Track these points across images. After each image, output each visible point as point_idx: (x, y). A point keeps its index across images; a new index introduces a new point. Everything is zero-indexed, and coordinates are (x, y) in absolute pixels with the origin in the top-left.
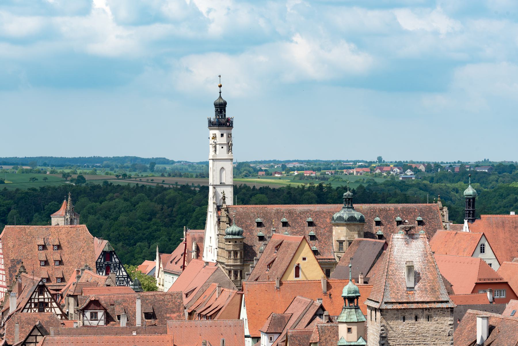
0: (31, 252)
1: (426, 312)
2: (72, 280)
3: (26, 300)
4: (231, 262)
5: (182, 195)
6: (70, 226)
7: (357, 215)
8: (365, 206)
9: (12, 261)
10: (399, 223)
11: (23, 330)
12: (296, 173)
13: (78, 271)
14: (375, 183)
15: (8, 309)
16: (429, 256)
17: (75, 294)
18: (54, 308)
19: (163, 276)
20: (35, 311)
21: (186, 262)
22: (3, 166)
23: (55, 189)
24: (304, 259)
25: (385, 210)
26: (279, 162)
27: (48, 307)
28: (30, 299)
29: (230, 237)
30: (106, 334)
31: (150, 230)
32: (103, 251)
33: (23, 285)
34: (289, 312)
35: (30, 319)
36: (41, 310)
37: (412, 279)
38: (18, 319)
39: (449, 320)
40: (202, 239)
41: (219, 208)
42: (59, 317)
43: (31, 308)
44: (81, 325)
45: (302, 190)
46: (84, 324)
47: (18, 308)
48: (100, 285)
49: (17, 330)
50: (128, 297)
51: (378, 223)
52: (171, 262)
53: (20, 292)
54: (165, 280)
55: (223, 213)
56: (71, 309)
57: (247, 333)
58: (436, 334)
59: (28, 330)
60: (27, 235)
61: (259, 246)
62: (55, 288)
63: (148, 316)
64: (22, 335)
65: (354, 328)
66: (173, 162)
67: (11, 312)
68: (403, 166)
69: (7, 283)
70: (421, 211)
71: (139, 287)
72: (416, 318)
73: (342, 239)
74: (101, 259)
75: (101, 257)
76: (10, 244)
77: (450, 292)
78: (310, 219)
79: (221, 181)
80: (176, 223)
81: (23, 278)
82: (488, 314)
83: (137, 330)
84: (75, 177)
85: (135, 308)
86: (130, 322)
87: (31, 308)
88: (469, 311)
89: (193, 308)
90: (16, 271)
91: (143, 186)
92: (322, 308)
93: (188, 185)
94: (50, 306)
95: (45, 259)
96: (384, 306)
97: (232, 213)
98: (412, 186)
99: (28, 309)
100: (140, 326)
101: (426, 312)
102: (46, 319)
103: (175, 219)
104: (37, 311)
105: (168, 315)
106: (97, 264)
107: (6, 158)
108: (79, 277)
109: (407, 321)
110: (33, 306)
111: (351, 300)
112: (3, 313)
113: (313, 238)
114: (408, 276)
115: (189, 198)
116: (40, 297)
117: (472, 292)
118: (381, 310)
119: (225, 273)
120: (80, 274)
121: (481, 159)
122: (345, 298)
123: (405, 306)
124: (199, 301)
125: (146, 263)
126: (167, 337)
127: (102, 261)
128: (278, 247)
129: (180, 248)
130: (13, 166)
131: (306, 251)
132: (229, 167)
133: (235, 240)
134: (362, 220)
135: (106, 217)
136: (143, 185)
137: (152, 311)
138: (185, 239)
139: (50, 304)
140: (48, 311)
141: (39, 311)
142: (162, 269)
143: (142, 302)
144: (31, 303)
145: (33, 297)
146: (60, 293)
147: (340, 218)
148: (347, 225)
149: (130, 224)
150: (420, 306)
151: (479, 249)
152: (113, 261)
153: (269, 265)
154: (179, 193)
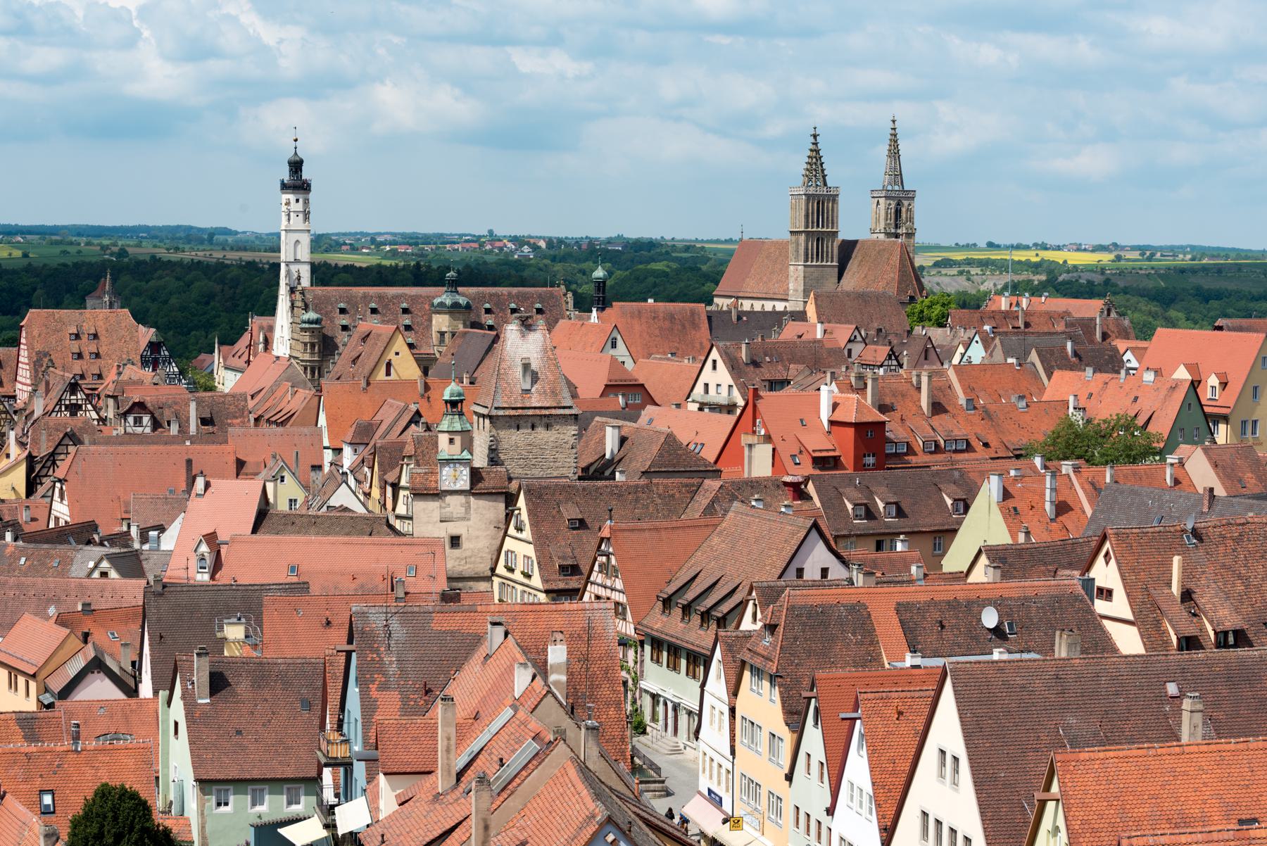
1: (546, 420)
2: (111, 376)
3: (55, 401)
4: (307, 357)
7: (462, 301)
8: (472, 290)
9: (38, 353)
10: (514, 311)
12: (388, 248)
13: (119, 366)
14: (485, 263)
16: (550, 352)
23: (90, 265)
24: (397, 354)
25: (496, 295)
26: (366, 234)
28: (60, 400)
29: (307, 326)
30: (153, 443)
34: (378, 418)
36: (73, 414)
37: (529, 379)
39: (572, 430)
40: (271, 329)
41: (292, 291)
45: (395, 269)
48: (146, 383)
49: (44, 438)
51: (488, 311)
53: (48, 391)
55: (298, 296)
56: (110, 414)
57: (326, 443)
58: (557, 447)
61: (341, 338)
63: (205, 421)
65: (458, 439)
66: (236, 233)
67: (36, 416)
68: (519, 241)
70: (540, 296)
71: (194, 387)
72: (533, 427)
73: (444, 329)
76: (36, 333)
77: (574, 396)
78: (405, 305)
79: (295, 257)
80: (240, 308)
82: (620, 423)
83: (191, 438)
84: (115, 249)
86: (183, 429)
88: (597, 419)
89: (260, 413)
92: (418, 413)
96: (494, 412)
97: (309, 297)
98: (530, 266)
101: (545, 419)
108: (119, 374)
109: (521, 431)
111: (454, 404)
113: (408, 328)
114: (524, 376)
117: (601, 396)
118: (490, 417)
119: (300, 369)
121: (614, 235)
122: (446, 402)
123: (520, 412)
124: (268, 405)
125: (203, 356)
126: (228, 448)
128: (365, 338)
130: (37, 237)
131: (400, 344)
132: (305, 240)
133: (312, 331)
134: (468, 307)
135: (153, 300)
143: (198, 404)
147: (442, 304)
148: (450, 313)
150: (538, 412)
151: (609, 343)
153: (354, 361)
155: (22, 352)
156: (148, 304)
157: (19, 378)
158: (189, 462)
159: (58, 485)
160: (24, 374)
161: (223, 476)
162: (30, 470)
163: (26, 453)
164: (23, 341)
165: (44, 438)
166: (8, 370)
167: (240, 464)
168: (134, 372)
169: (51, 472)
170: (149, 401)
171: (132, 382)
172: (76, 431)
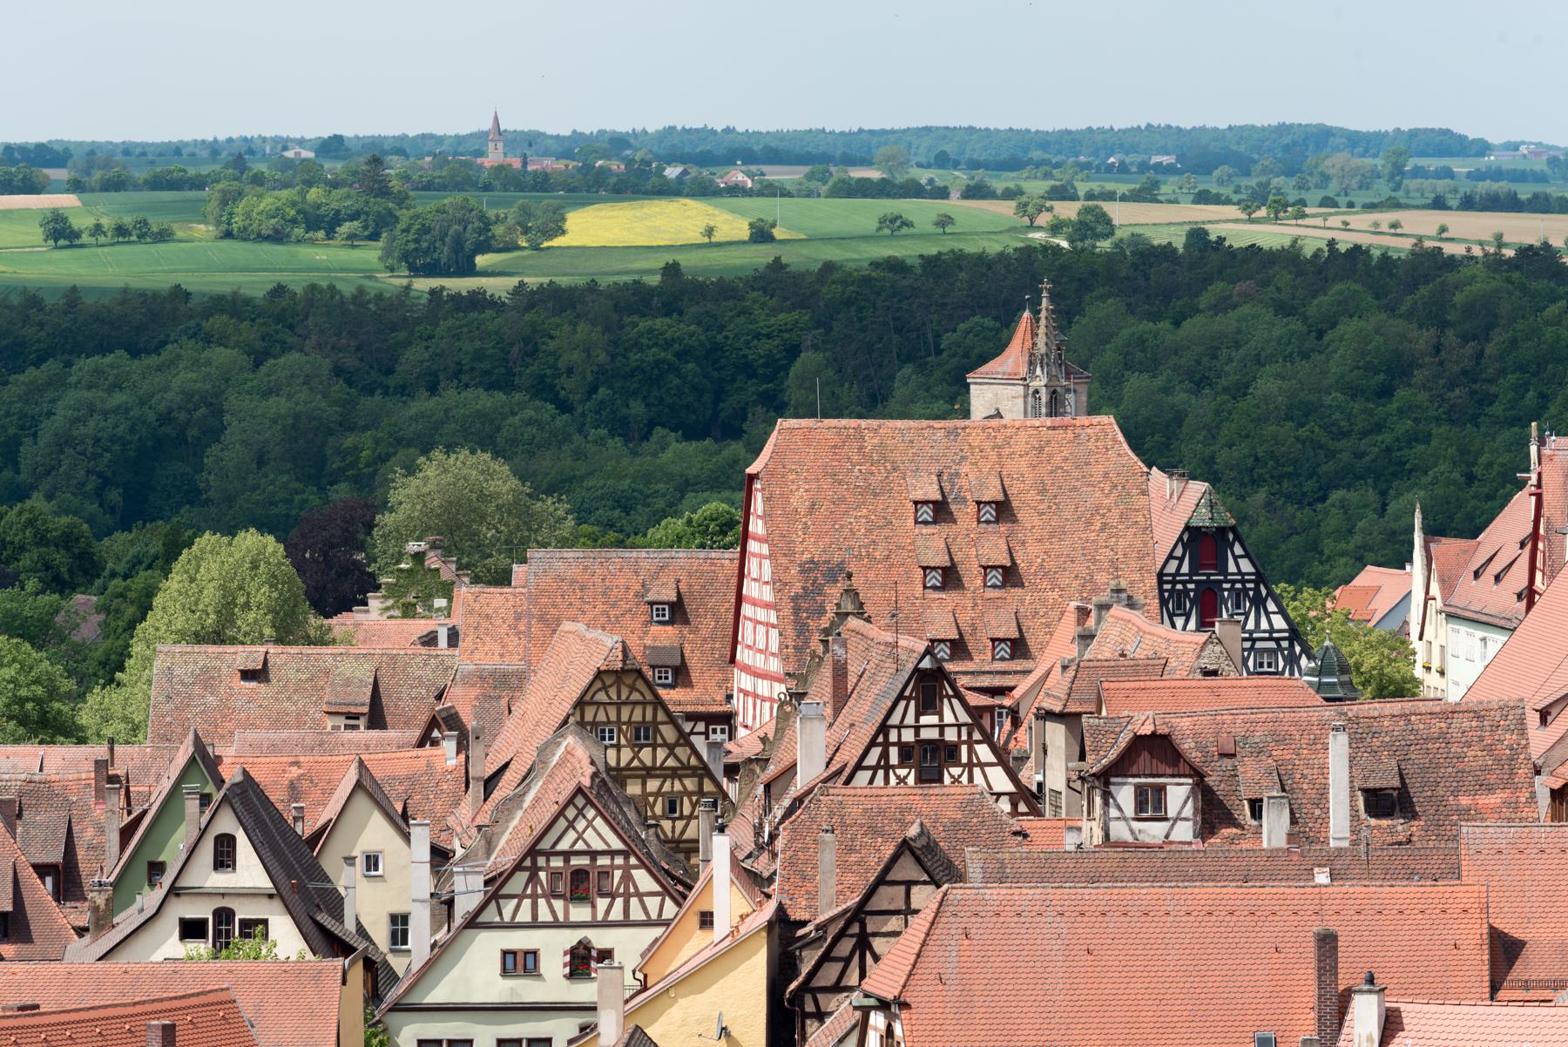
0: (886, 532)
2: (1056, 647)
5: (1523, 288)
6: (1049, 422)
9: (808, 568)
11: (853, 858)
13: (1083, 613)
15: (791, 769)
17: (1072, 708)
18: (982, 765)
19: (1442, 632)
20: (901, 780)
21: (1539, 575)
22: (765, 168)
23: (981, 260)
27: (959, 764)
28: (884, 728)
31: (1386, 438)
32: (1187, 528)
33: (853, 670)
35: (882, 812)
38: (832, 814)
42: (1005, 805)
43: (888, 768)
44: (1098, 837)
46: (1107, 836)
47: (833, 769)
48: (1170, 669)
50: (1295, 723)
52: (1477, 575)
53: (841, 697)
54: (1449, 651)
56: (1056, 774)
59: (873, 860)
60: (867, 457)
62: (985, 681)
63: (1382, 802)
64: (850, 879)
66: (1483, 148)
67: (800, 783)
69: (785, 659)
71: (1341, 681)
74: (1181, 560)
75: (1179, 552)
76: (800, 500)
80: (1497, 409)
81: (853, 642)
84: (1068, 210)
85: (1323, 770)
86: (1305, 829)
87: (888, 768)
90: (821, 611)
91: (1357, 249)
93: (1546, 246)
94: (964, 759)
95: (944, 561)
99: (875, 769)
100: (1346, 844)
102: (951, 813)
103: (1493, 389)
104: (911, 780)
105: (1465, 801)
106: (1161, 582)
107: (780, 136)
108: (1086, 638)
110: (894, 757)
112: (768, 787)
115: (1554, 300)
116: (924, 720)
120: (1091, 622)
125: (1370, 576)
126: (1461, 895)
127: (1185, 569)
129: (1516, 517)
130: (807, 169)
135: (1200, 382)
136: (1357, 248)
137: (1396, 783)
138: (1534, 477)
139: (964, 748)
140: (956, 780)
141: (920, 780)
142: (1439, 604)
143: (1356, 742)
144: (886, 745)
145: (895, 719)
146: (1007, 702)
149: (1300, 412)
152: (1232, 568)
154: (1509, 280)
155: (752, 566)
156: (1180, 397)
157: (743, 655)
158: (1327, 943)
159: (878, 1020)
160: (762, 640)
161: (1441, 994)
162: (781, 969)
163: (770, 909)
164: (757, 526)
165: (828, 858)
166: (706, 625)
167: (1505, 951)
168: (1137, 631)
169: (853, 978)
170: (1188, 734)
171: (1126, 666)
172: (938, 834)
